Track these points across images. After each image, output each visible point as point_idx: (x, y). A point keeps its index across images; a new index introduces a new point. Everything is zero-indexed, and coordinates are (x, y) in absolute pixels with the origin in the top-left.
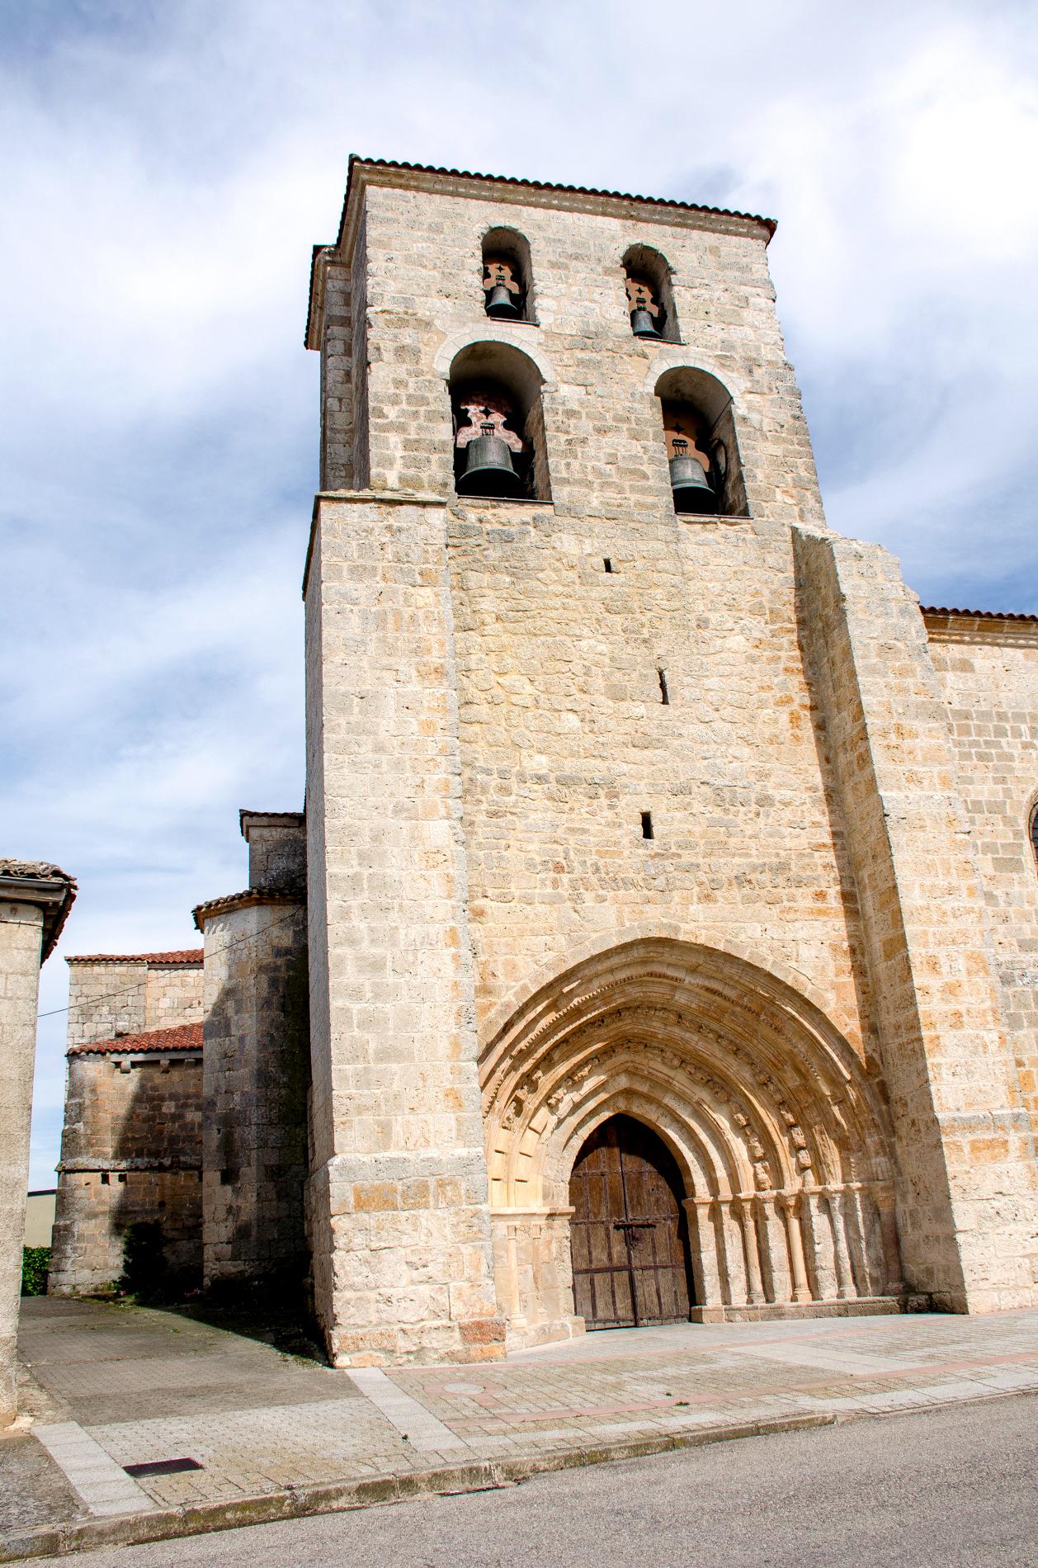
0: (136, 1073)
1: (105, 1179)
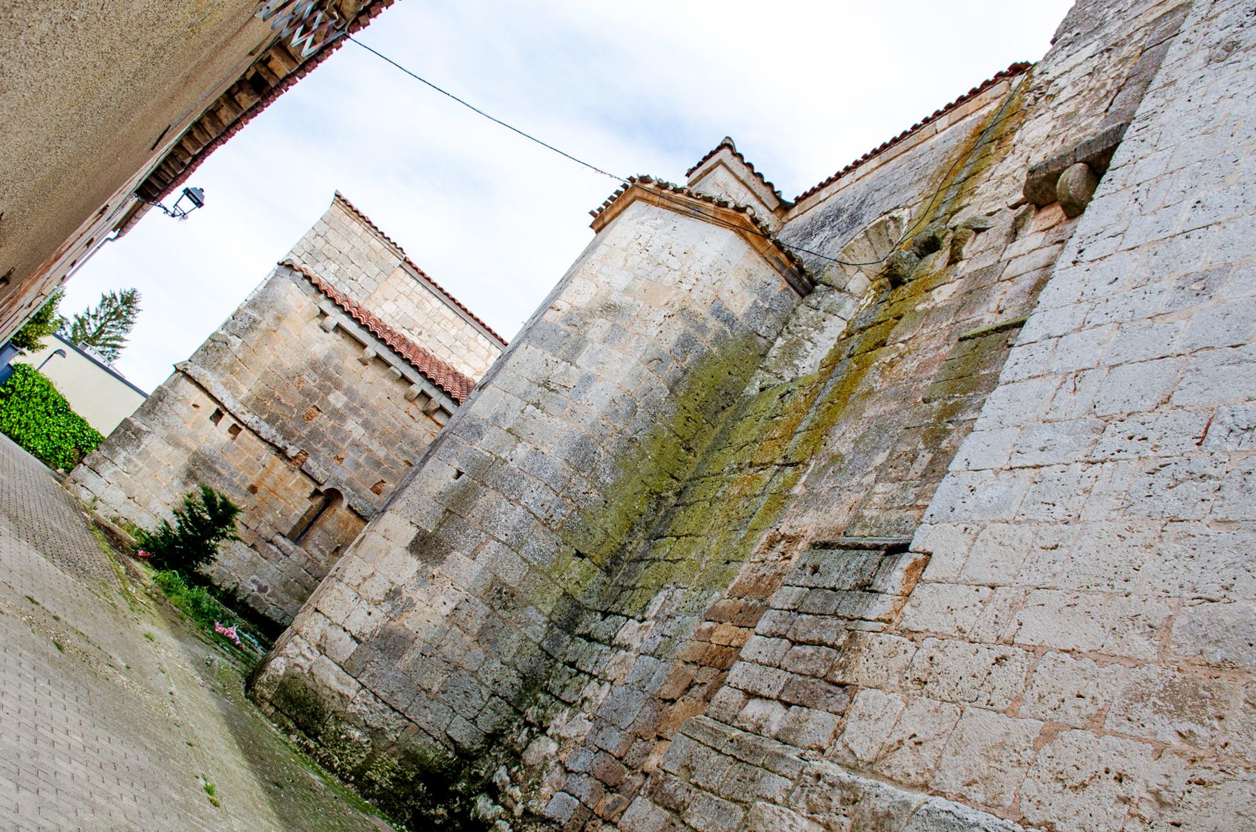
0: (334, 339)
1: (218, 416)
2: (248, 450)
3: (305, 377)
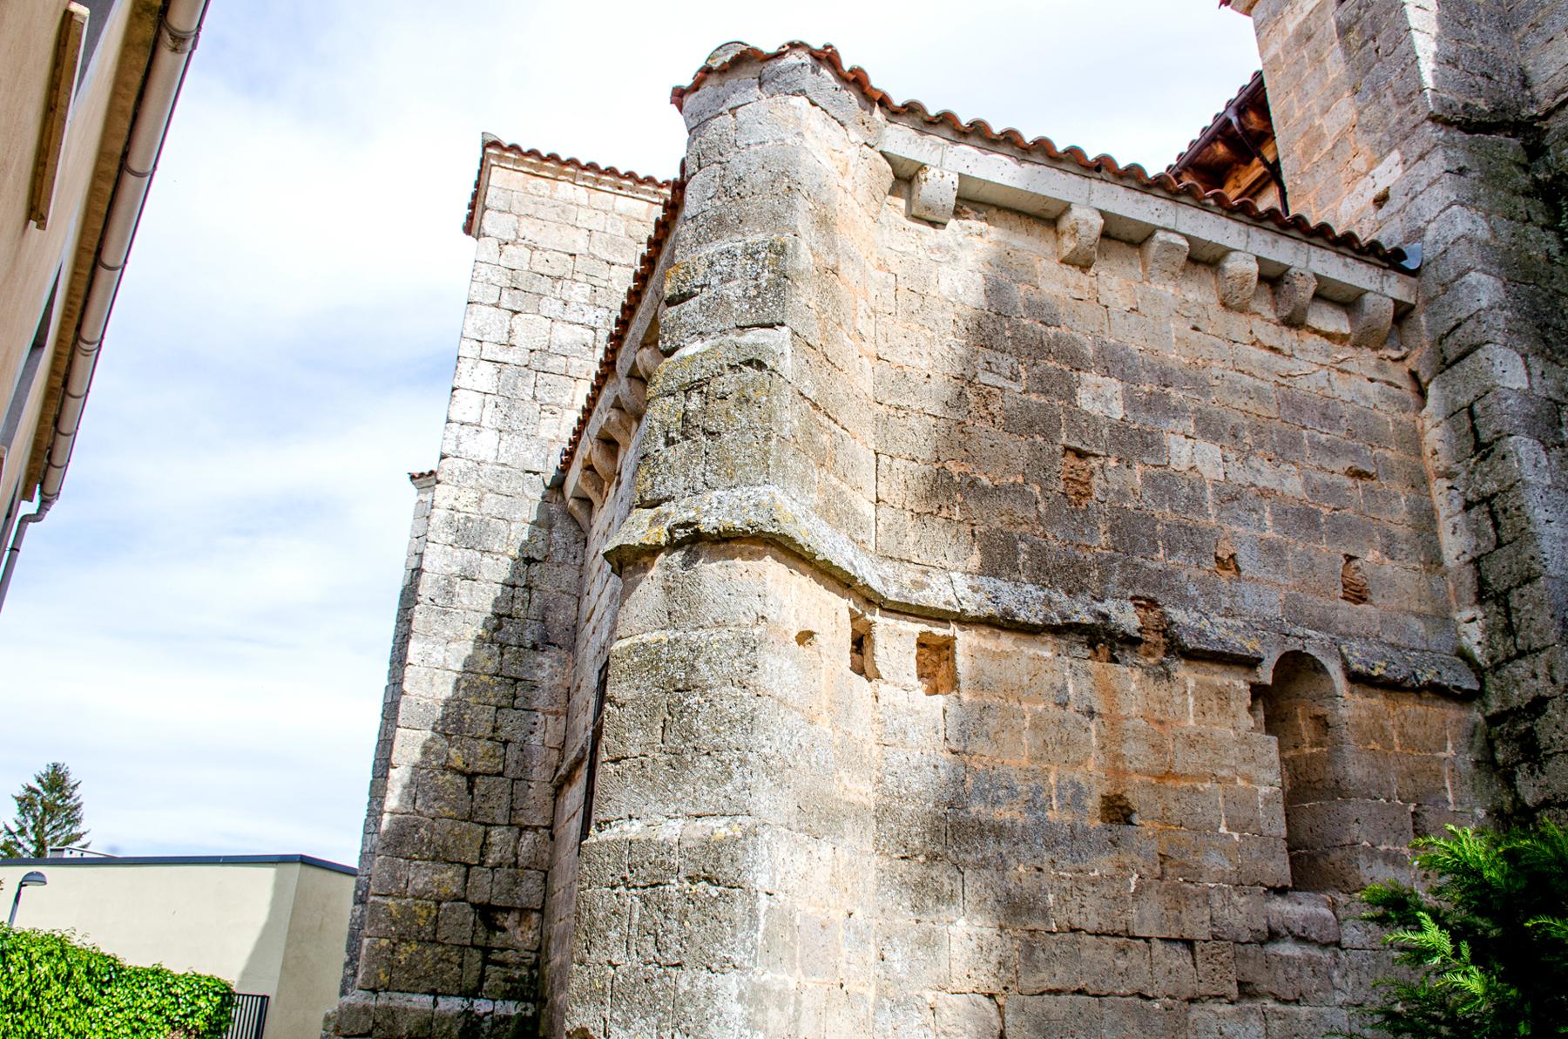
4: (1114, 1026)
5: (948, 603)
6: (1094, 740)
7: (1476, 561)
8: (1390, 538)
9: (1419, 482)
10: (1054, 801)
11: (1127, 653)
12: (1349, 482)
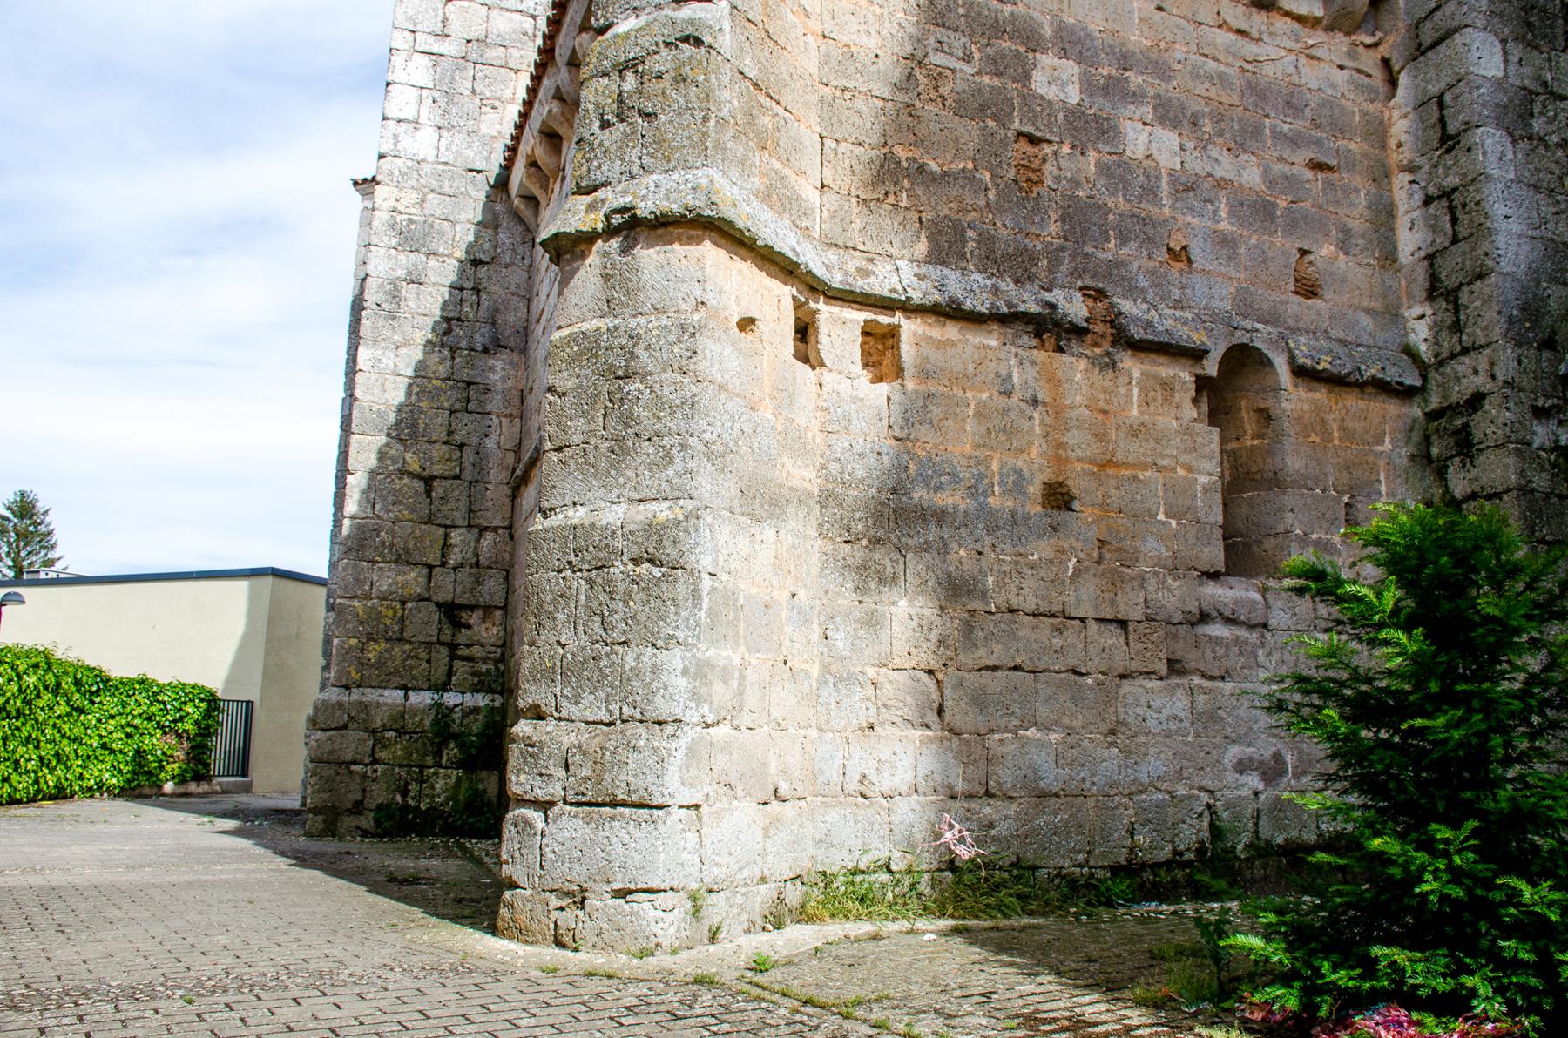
2: (961, 379)
3: (937, 59)
4: (1048, 699)
5: (894, 291)
6: (1037, 429)
7: (1430, 257)
8: (1346, 232)
9: (1381, 176)
10: (996, 488)
11: (1074, 343)
12: (1309, 174)
